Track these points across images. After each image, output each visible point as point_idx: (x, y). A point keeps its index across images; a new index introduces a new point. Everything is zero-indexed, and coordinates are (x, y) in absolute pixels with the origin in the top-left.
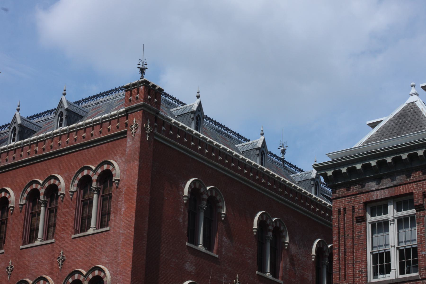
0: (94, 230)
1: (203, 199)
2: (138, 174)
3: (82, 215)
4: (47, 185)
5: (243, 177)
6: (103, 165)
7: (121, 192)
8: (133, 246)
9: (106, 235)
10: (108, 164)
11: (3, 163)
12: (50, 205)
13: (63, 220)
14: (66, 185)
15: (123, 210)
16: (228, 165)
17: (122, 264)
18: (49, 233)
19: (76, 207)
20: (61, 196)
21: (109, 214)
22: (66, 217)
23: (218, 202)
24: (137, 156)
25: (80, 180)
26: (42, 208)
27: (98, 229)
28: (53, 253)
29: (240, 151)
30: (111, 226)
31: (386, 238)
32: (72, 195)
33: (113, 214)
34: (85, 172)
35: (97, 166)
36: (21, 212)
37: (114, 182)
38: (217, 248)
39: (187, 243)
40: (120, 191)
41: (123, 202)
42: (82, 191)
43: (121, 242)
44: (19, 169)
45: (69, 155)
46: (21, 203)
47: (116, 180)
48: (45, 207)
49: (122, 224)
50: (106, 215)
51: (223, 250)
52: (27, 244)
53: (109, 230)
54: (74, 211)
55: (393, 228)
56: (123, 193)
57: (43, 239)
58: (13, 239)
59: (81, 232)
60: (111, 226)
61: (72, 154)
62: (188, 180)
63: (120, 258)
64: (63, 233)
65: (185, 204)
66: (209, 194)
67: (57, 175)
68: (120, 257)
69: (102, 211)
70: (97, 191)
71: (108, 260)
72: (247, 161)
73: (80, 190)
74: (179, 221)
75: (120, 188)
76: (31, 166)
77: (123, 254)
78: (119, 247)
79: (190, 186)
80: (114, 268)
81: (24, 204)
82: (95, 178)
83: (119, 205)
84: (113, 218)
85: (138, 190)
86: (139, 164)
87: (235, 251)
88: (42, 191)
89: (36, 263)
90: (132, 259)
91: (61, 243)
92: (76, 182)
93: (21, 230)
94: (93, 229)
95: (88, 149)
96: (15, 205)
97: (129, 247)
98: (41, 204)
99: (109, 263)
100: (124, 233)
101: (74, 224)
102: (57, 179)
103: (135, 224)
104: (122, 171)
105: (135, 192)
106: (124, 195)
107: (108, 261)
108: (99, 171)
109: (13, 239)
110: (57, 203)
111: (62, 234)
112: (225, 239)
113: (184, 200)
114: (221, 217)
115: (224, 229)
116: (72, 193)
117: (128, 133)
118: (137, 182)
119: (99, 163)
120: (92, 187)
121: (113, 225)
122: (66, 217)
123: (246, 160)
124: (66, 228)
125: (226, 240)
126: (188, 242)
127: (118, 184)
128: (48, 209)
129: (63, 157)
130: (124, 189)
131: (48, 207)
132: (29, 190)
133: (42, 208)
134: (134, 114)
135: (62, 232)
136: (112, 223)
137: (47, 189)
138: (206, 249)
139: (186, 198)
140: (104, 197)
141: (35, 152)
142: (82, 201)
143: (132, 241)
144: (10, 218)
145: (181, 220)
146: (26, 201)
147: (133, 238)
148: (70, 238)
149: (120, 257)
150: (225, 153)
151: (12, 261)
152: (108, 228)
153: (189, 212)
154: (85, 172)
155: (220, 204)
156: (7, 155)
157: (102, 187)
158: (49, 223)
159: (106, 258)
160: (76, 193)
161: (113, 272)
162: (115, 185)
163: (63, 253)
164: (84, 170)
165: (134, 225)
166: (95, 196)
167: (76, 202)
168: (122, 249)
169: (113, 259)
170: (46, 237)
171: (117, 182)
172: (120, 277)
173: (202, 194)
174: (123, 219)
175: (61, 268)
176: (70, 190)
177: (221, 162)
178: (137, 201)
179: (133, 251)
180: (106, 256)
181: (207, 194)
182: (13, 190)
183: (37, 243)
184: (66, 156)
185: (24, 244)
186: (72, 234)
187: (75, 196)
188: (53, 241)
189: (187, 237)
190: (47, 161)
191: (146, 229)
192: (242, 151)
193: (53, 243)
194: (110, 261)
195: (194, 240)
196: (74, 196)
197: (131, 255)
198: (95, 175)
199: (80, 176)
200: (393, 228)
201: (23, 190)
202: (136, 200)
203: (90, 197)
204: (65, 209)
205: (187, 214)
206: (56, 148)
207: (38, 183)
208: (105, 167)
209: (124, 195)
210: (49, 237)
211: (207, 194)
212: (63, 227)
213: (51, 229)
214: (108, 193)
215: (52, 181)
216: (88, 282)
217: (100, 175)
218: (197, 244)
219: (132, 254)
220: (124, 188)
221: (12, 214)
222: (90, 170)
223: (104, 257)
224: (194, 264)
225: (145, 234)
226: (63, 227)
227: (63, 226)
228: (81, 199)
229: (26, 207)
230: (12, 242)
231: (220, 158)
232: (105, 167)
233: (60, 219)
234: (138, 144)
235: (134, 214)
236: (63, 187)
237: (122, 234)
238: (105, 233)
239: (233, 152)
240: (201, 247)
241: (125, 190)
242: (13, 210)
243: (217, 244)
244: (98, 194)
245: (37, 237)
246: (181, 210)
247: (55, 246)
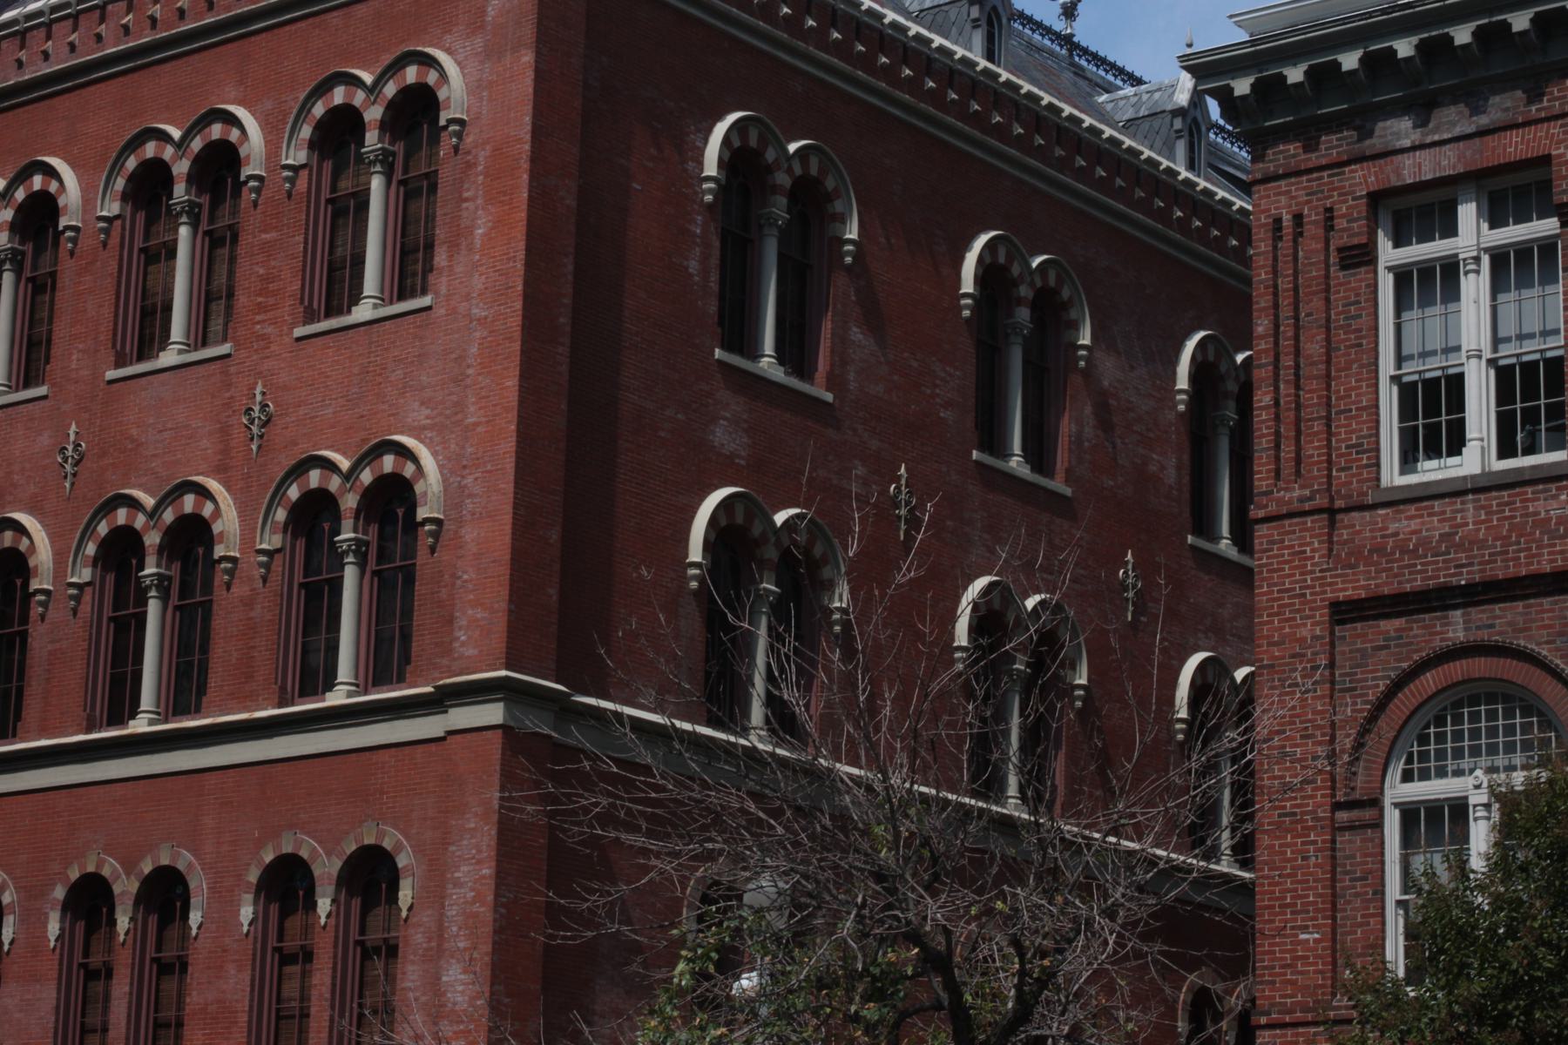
0: (375, 306)
1: (775, 189)
2: (531, 97)
3: (331, 253)
4: (197, 144)
5: (922, 105)
6: (404, 67)
7: (470, 165)
8: (521, 365)
9: (419, 327)
10: (420, 63)
11: (34, 68)
12: (211, 220)
13: (261, 271)
14: (266, 142)
15: (480, 231)
16: (867, 62)
17: (480, 429)
18: (212, 323)
19: (307, 224)
20: (252, 184)
21: (430, 247)
22: (273, 263)
23: (829, 198)
24: (529, 31)
25: (320, 126)
26: (184, 231)
27: (391, 303)
28: (227, 395)
29: (911, 9)
30: (437, 294)
31: (1450, 325)
32: (292, 181)
33: (445, 248)
34: (339, 96)
35: (379, 70)
36: (105, 244)
37: (445, 128)
38: (828, 368)
39: (717, 350)
40: (468, 162)
41: (479, 201)
42: (328, 166)
43: (474, 350)
44: (92, 89)
45: (276, 31)
46: (104, 213)
47: (451, 121)
48: (195, 226)
49: (478, 283)
50: (418, 250)
51: (852, 376)
52: (131, 364)
53: (429, 308)
54: (301, 238)
55: (1475, 287)
56: (480, 168)
57: (188, 345)
58: (81, 346)
59: (328, 315)
60: (437, 294)
61: (287, 28)
62: (720, 117)
63: (472, 409)
64: (264, 321)
65: (710, 206)
66: (798, 170)
67: (232, 108)
68: (473, 404)
69: (403, 236)
70: (381, 162)
71: (427, 418)
72: (934, 45)
73: (322, 159)
74: (686, 268)
75: (469, 153)
76: (136, 75)
78: (469, 367)
79: (726, 141)
80: (453, 446)
81: (117, 217)
82: (373, 114)
83: (465, 214)
84: (444, 263)
85: (534, 160)
86: (536, 61)
87: (896, 378)
88: (181, 168)
90: (515, 413)
91: (255, 357)
92: (306, 132)
93: (107, 312)
94: (371, 306)
95: (346, 10)
96: (83, 221)
97: (505, 369)
98: (179, 214)
99: (431, 428)
100: (486, 318)
101: (303, 286)
102: (232, 120)
103: (526, 284)
104: (474, 89)
105: (525, 165)
106: (481, 177)
107: (428, 421)
108: (390, 90)
109: (81, 346)
110: (235, 212)
111: (258, 323)
112: (856, 334)
113: (704, 192)
114: (842, 256)
115: (853, 298)
116: (290, 174)
118: (529, 128)
119: (387, 59)
120: (363, 150)
121: (443, 290)
122: (273, 263)
123: (932, 41)
124: (271, 301)
125: (861, 336)
126: (723, 347)
127: (459, 135)
128: (206, 233)
129: (253, 39)
130: (482, 156)
131: (204, 226)
132: (131, 163)
133: (184, 231)
135: (258, 318)
136: (440, 282)
137: (198, 160)
138: (786, 373)
139: (712, 185)
140: (410, 186)
141: (149, 22)
142: (328, 201)
143: (517, 346)
144: (67, 269)
145: (693, 266)
146: (122, 209)
147: (517, 335)
148: (287, 340)
149: (473, 404)
150: (852, 17)
151: (77, 427)
152: (426, 301)
153: (725, 236)
154: (339, 96)
155: (838, 206)
156: (49, 37)
157: (399, 148)
158: (208, 283)
159: (423, 408)
160: (304, 174)
161: (449, 459)
162: (447, 142)
163: (264, 394)
164: (331, 89)
165: (520, 288)
166: (376, 184)
167: (308, 207)
168: (479, 374)
169: (448, 412)
170: (200, 335)
171: (457, 128)
172: (476, 479)
173: (769, 169)
174: (482, 265)
175: (259, 447)
176: (284, 162)
177: (841, 50)
178: (530, 197)
179: (520, 381)
180: (422, 404)
181: (790, 171)
182: (74, 165)
183: (168, 358)
184: (264, 35)
185: (119, 364)
186: (294, 325)
187: (302, 183)
188: (225, 349)
189: (719, 330)
190: (196, 57)
191: (565, 301)
192: (918, 8)
193: (228, 356)
194: (437, 420)
195: (743, 339)
196: (298, 182)
197: (512, 397)
198: (373, 103)
199: (319, 110)
200: (1475, 287)
201: (109, 165)
202: (530, 196)
203: (357, 186)
204: (265, 231)
205: (717, 243)
207: (164, 137)
208: (411, 74)
209: (481, 177)
210: (211, 336)
211: (790, 171)
212: (260, 299)
213: (218, 307)
214: (423, 171)
215: (216, 131)
217: (391, 106)
218: (755, 355)
219: (517, 394)
220: (484, 149)
221: (72, 253)
222: (354, 85)
223: (417, 403)
224: (745, 426)
225: (562, 320)
226: (260, 299)
227: (260, 295)
228: (326, 194)
229: (123, 228)
230: (74, 357)
231: (836, 35)
232: (411, 74)
233: (250, 270)
235: (522, 245)
236: (257, 150)
237: (479, 320)
239: (885, 11)
240: (768, 364)
241: (486, 158)
242: (74, 240)
243: (828, 354)
244: (388, 175)
245: (168, 337)
246: (692, 228)
247: (233, 369)
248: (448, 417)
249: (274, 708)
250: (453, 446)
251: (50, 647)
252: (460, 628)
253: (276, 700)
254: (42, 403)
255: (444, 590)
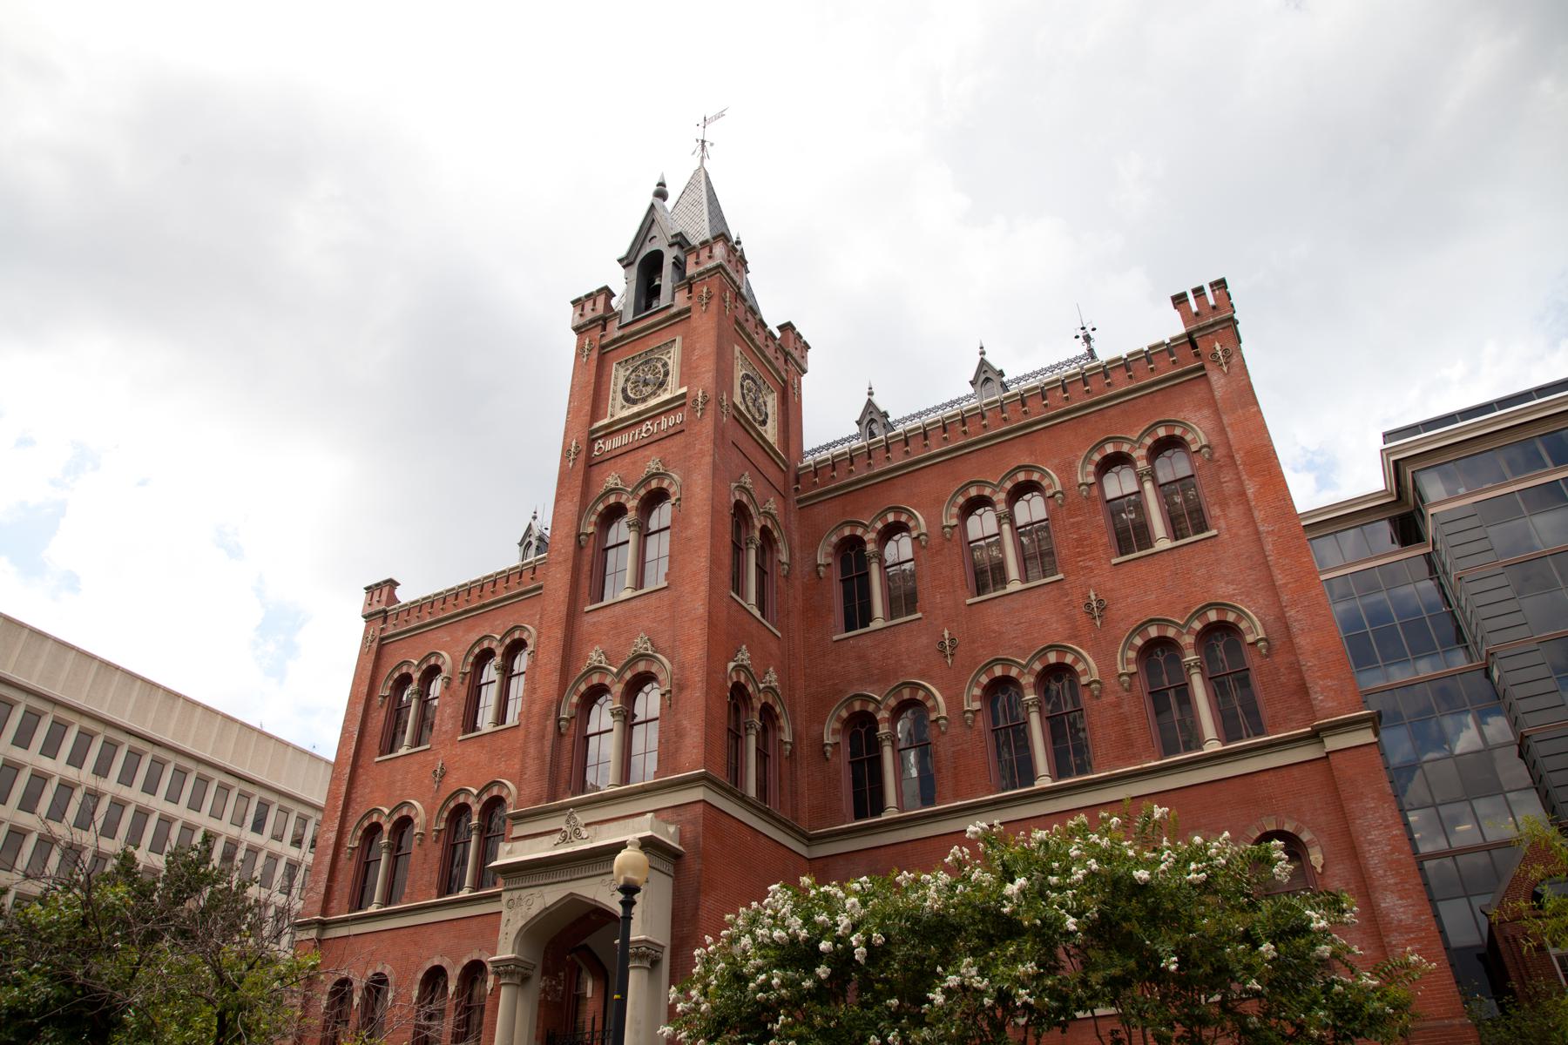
13: (1075, 536)
17: (1290, 586)
28: (1066, 600)
64: (1084, 560)
68: (1280, 574)
71: (1235, 590)
77: (1286, 567)
80: (1261, 601)
89: (1022, 623)
99: (1241, 594)
100: (1273, 530)
117: (1207, 366)
124: (1087, 549)
134: (1210, 336)
152: (1214, 532)
175: (1102, 623)
186: (1113, 557)
188: (1060, 576)
194: (1243, 590)
206: (1019, 420)
216: (1194, 637)
223: (1223, 585)
226: (1078, 550)
227: (1077, 548)
234: (1243, 380)
238: (1209, 543)
248: (1250, 587)
249: (1156, 761)
250: (1261, 601)
251: (953, 749)
252: (1316, 693)
253: (1158, 756)
254: (917, 622)
255: (1282, 677)
